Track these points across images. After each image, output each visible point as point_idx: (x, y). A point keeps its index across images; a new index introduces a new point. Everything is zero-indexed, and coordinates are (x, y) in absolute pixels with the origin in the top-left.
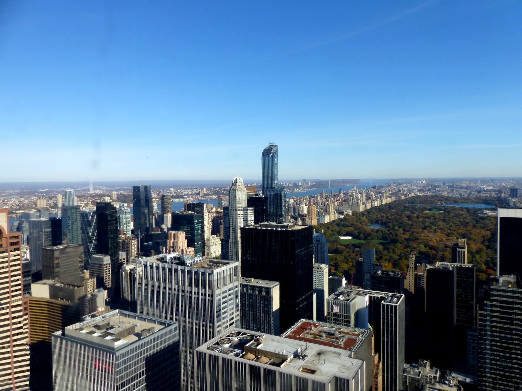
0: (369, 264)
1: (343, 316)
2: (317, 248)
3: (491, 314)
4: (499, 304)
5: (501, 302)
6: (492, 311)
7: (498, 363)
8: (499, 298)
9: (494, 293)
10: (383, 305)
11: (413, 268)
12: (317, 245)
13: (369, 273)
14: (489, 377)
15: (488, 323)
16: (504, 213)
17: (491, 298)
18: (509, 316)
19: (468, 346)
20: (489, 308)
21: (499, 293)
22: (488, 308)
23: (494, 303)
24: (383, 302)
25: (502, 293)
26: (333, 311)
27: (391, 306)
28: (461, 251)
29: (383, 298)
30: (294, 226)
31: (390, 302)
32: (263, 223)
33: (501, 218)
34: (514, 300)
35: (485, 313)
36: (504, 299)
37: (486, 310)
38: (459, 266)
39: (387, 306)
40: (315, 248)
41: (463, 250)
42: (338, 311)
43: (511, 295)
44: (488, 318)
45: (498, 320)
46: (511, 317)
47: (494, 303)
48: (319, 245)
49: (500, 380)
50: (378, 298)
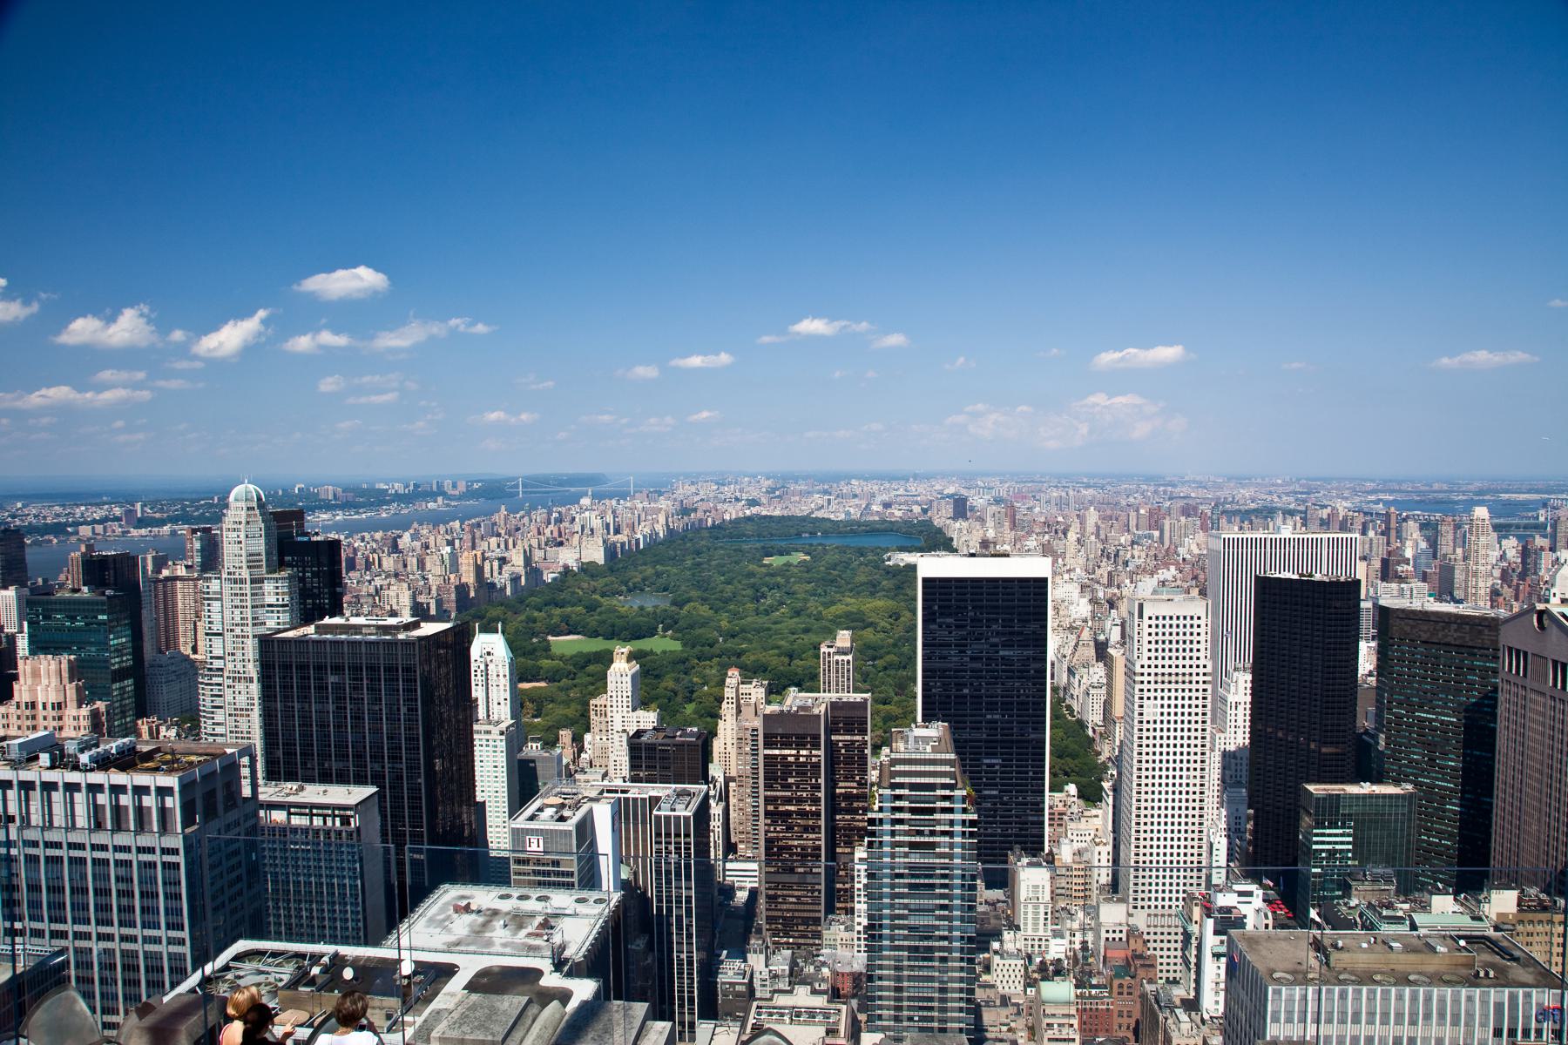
0: (625, 709)
1: (556, 863)
4: (906, 792)
5: (913, 787)
6: (895, 809)
7: (906, 922)
9: (898, 768)
10: (658, 818)
13: (624, 731)
14: (888, 957)
15: (887, 838)
16: (932, 566)
19: (857, 886)
23: (898, 792)
24: (655, 812)
25: (913, 768)
27: (677, 818)
29: (655, 801)
30: (415, 625)
32: (327, 620)
33: (925, 580)
35: (881, 815)
37: (881, 809)
39: (668, 818)
41: (846, 658)
43: (932, 768)
44: (887, 827)
45: (906, 827)
47: (898, 792)
49: (909, 959)
50: (643, 800)
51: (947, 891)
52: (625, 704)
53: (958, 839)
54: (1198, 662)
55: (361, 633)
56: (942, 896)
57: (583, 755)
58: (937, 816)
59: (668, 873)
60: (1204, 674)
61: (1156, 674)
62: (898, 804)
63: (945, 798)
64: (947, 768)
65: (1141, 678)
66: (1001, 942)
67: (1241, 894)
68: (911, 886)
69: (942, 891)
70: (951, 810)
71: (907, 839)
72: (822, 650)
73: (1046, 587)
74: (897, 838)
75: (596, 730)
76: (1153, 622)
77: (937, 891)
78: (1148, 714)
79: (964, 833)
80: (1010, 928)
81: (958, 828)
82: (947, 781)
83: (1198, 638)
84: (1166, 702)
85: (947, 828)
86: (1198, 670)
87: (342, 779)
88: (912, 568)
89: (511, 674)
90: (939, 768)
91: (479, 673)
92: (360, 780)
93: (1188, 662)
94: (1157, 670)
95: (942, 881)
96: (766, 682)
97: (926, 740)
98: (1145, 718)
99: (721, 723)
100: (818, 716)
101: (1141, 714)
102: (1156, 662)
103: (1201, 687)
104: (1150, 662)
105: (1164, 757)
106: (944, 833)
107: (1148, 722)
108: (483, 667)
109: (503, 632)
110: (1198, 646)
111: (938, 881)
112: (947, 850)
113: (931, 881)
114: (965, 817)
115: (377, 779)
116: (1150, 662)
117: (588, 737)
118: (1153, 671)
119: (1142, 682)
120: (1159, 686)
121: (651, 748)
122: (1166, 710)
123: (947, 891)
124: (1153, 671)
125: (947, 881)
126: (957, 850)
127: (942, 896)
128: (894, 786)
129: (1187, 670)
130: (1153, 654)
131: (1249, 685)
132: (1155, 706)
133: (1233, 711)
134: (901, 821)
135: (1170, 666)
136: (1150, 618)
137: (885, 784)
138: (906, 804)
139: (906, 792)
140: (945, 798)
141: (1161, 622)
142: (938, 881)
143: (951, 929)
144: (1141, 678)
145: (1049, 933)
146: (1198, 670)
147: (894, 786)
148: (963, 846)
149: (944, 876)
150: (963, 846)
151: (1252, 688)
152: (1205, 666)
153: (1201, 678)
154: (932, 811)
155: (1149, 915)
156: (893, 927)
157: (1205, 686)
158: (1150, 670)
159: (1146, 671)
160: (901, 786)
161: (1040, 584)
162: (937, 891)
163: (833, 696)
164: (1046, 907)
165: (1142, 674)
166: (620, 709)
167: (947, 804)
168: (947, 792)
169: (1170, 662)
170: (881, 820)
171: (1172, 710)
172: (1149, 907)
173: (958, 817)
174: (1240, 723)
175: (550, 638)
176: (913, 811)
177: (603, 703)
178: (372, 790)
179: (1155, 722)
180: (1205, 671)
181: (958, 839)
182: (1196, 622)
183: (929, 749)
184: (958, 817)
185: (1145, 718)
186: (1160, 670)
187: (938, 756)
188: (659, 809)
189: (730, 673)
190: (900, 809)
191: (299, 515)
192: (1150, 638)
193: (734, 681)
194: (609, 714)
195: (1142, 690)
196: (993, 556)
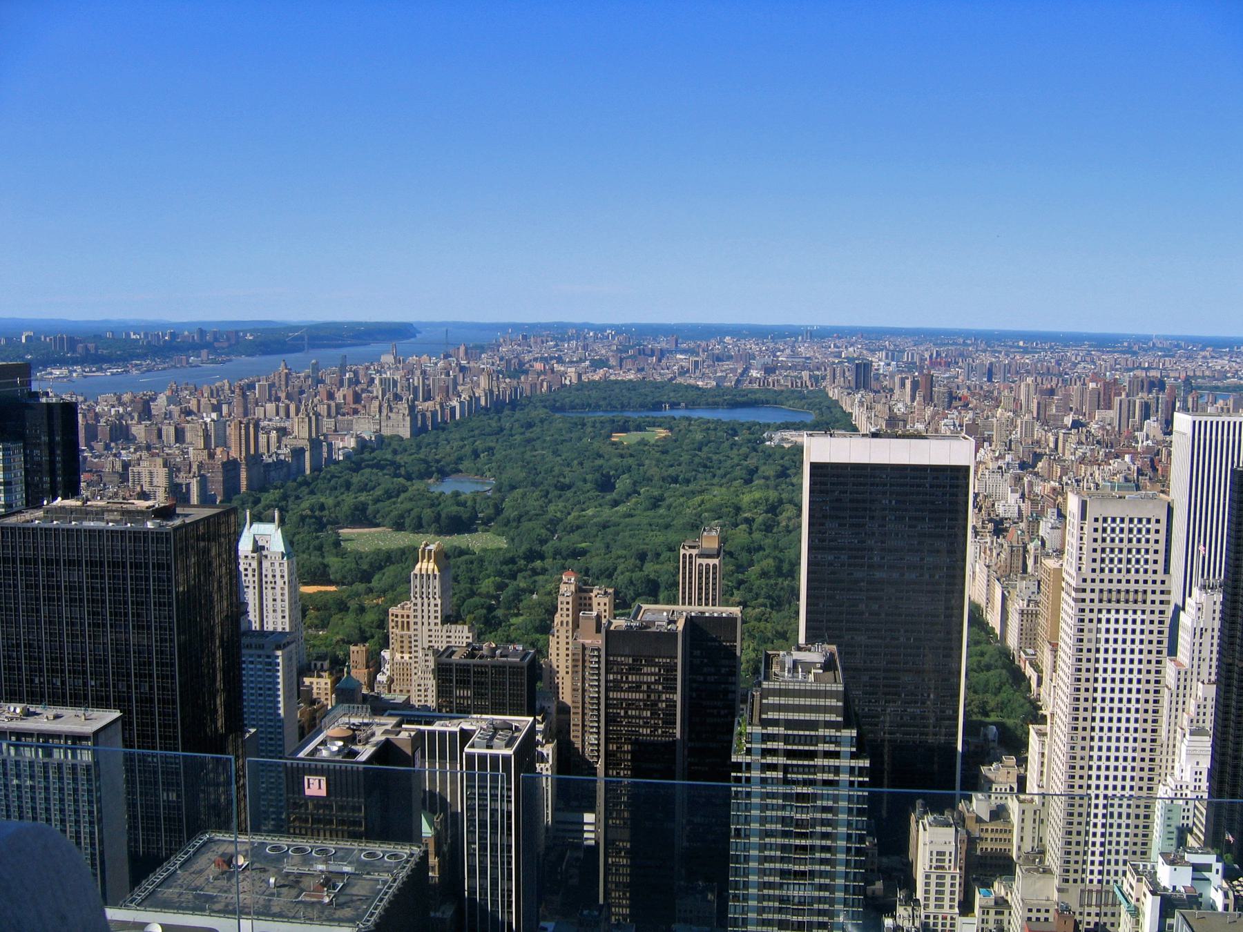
0: (432, 621)
2: (261, 574)
3: (764, 761)
4: (782, 731)
5: (789, 724)
6: (765, 752)
8: (782, 716)
9: (771, 700)
10: (470, 757)
11: (567, 622)
12: (260, 564)
17: (764, 716)
18: (806, 763)
20: (759, 746)
21: (783, 701)
22: (754, 746)
23: (770, 730)
24: (467, 750)
25: (791, 701)
26: (308, 792)
27: (495, 758)
28: (708, 565)
29: (466, 735)
31: (489, 747)
32: (59, 502)
33: (814, 466)
34: (821, 717)
35: (748, 759)
36: (796, 716)
37: (749, 752)
38: (693, 614)
39: (483, 758)
40: (254, 576)
41: (712, 562)
42: (323, 793)
43: (814, 702)
44: (755, 774)
46: (811, 763)
47: (770, 730)
48: (266, 564)
50: (453, 734)
51: (828, 856)
52: (432, 615)
53: (844, 792)
54: (1155, 577)
55: (102, 520)
56: (823, 862)
57: (380, 677)
58: (819, 762)
59: (483, 825)
60: (1162, 592)
61: (1101, 591)
62: (770, 745)
63: (830, 740)
64: (833, 702)
65: (1082, 595)
66: (894, 917)
67: (1197, 868)
68: (784, 848)
69: (823, 855)
70: (836, 755)
71: (781, 790)
72: (682, 552)
73: (967, 477)
74: (769, 789)
75: (397, 646)
76: (1099, 525)
77: (817, 855)
78: (1090, 641)
79: (852, 783)
80: (907, 904)
81: (844, 777)
82: (833, 718)
83: (1156, 547)
84: (1112, 626)
85: (831, 777)
86: (1154, 587)
87: (78, 699)
88: (798, 450)
89: (290, 574)
90: (822, 702)
91: (250, 572)
92: (101, 702)
93: (1141, 576)
94: (1102, 586)
95: (824, 843)
96: (610, 591)
97: (808, 666)
98: (1086, 645)
99: (553, 641)
100: (672, 635)
101: (1081, 640)
102: (1102, 576)
103: (1157, 607)
104: (1094, 576)
105: (1108, 695)
106: (827, 783)
107: (1089, 650)
108: (255, 564)
109: (282, 523)
110: (1156, 557)
111: (818, 842)
112: (830, 803)
113: (809, 842)
114: (853, 763)
115: (119, 702)
116: (1094, 576)
117: (386, 654)
118: (1097, 586)
119: (1083, 600)
120: (1105, 605)
121: (463, 669)
122: (1112, 636)
123: (828, 856)
124: (1097, 586)
125: (829, 843)
126: (843, 804)
127: (823, 862)
128: (765, 723)
129: (1141, 587)
130: (1097, 566)
131: (1218, 607)
132: (1099, 631)
133: (1197, 640)
134: (773, 767)
135: (1119, 581)
136: (1096, 520)
137: (756, 720)
138: (781, 745)
139: (782, 731)
140: (830, 740)
141: (1109, 525)
142: (818, 842)
143: (832, 902)
144: (1082, 595)
145: (957, 910)
146: (1154, 587)
147: (765, 723)
148: (850, 799)
149: (825, 836)
150: (850, 799)
151: (1222, 612)
152: (1163, 582)
153: (1158, 597)
154: (812, 755)
155: (1082, 891)
156: (762, 898)
157: (1162, 607)
158: (1093, 586)
159: (1088, 586)
160: (775, 723)
161: (960, 473)
162: (817, 855)
163: (695, 609)
164: (953, 878)
165: (1084, 590)
166: (426, 620)
167: (832, 748)
168: (832, 732)
169: (1120, 576)
170: (748, 765)
171: (1120, 636)
172: (1083, 880)
173: (845, 763)
174: (1206, 654)
175: (340, 531)
176: (789, 754)
177: (405, 612)
178: (116, 714)
179: (1098, 650)
180: (1163, 587)
181: (844, 792)
182: (1153, 526)
183: (811, 677)
184: (845, 763)
185: (1086, 645)
186: (1106, 586)
187: (822, 687)
188: (472, 746)
189: (565, 578)
190: (773, 752)
191: (25, 370)
192: (1095, 545)
193: (573, 588)
194: (412, 626)
195: (1083, 610)
196: (898, 437)
